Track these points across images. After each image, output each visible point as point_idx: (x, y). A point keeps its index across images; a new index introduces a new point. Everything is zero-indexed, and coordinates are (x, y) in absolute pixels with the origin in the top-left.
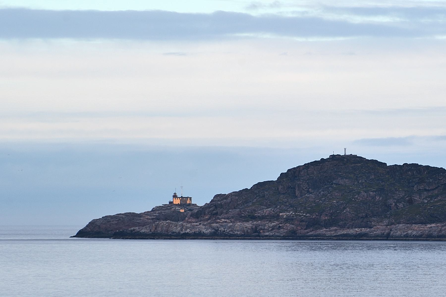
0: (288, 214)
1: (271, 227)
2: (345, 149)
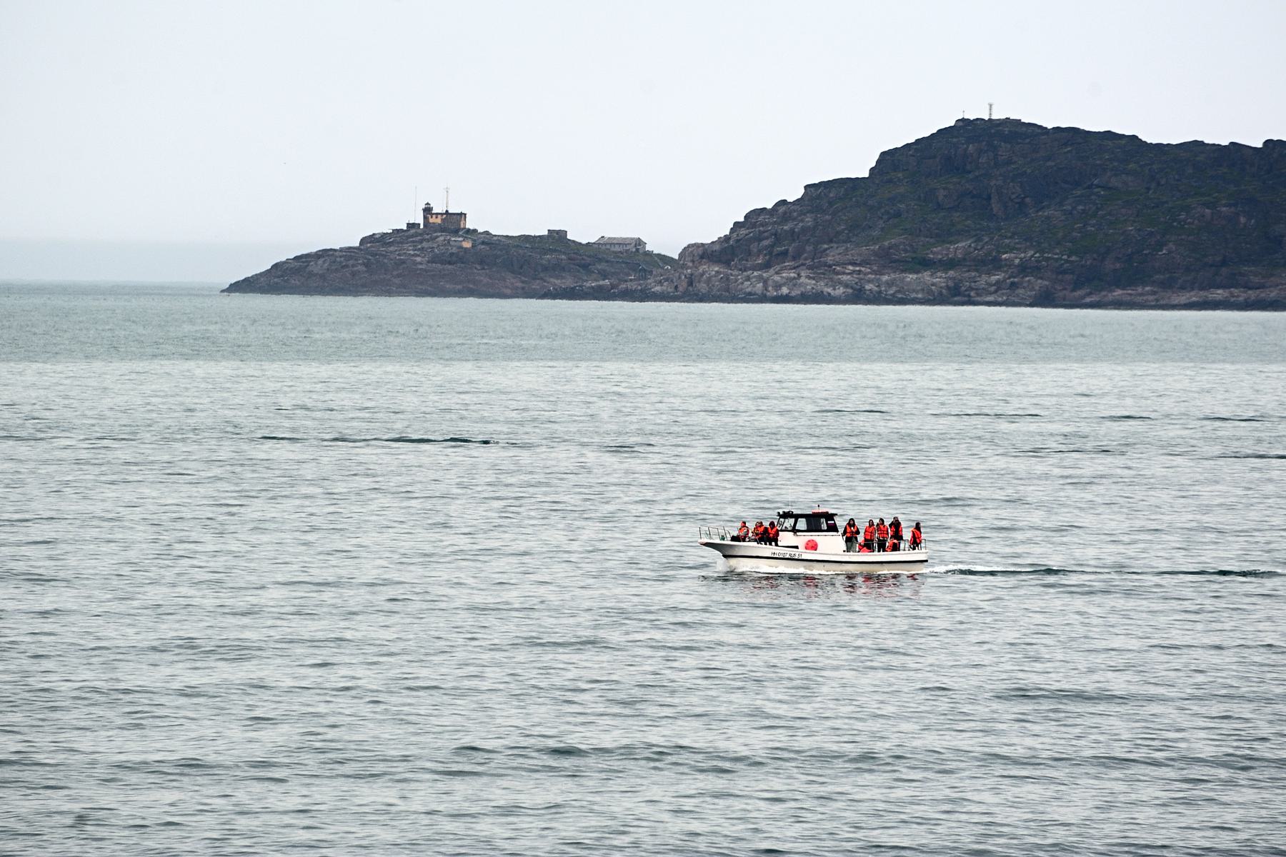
0: (1023, 255)
1: (994, 285)
2: (991, 106)
